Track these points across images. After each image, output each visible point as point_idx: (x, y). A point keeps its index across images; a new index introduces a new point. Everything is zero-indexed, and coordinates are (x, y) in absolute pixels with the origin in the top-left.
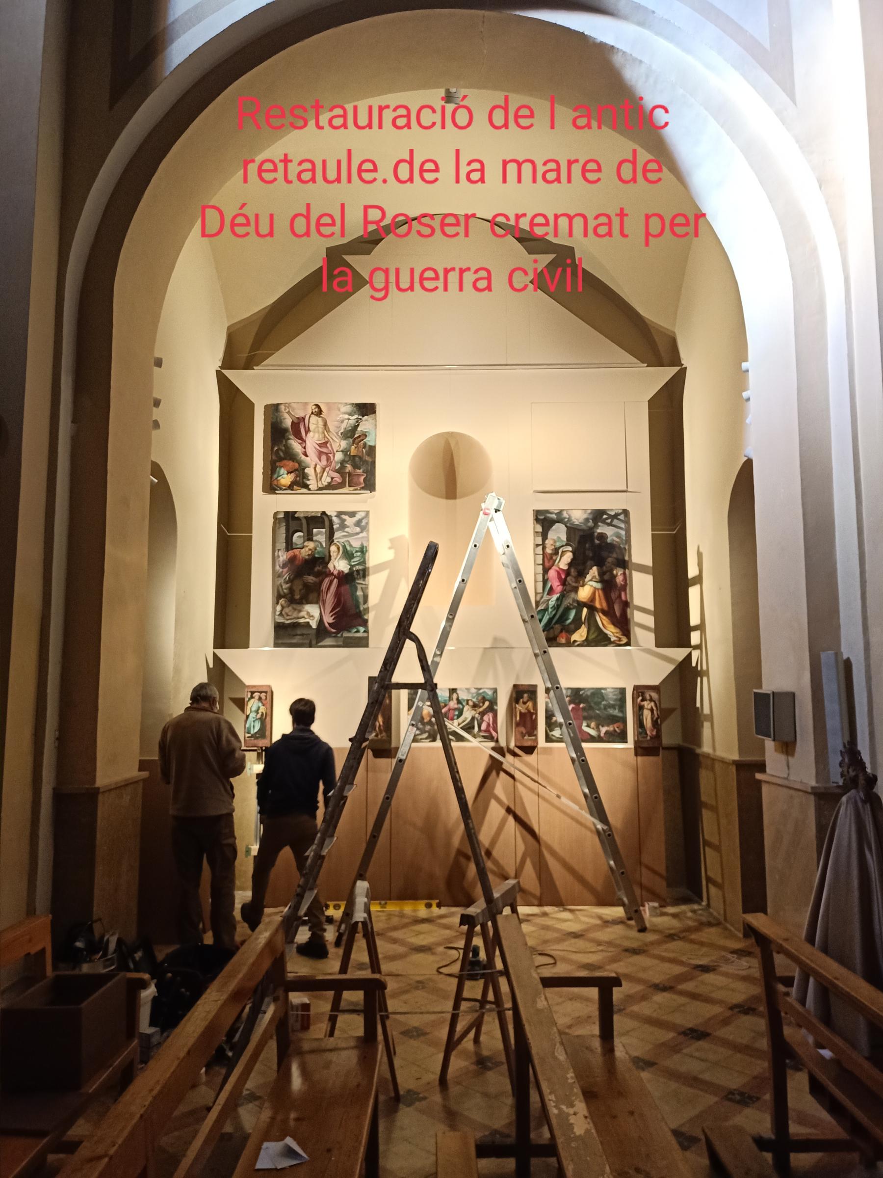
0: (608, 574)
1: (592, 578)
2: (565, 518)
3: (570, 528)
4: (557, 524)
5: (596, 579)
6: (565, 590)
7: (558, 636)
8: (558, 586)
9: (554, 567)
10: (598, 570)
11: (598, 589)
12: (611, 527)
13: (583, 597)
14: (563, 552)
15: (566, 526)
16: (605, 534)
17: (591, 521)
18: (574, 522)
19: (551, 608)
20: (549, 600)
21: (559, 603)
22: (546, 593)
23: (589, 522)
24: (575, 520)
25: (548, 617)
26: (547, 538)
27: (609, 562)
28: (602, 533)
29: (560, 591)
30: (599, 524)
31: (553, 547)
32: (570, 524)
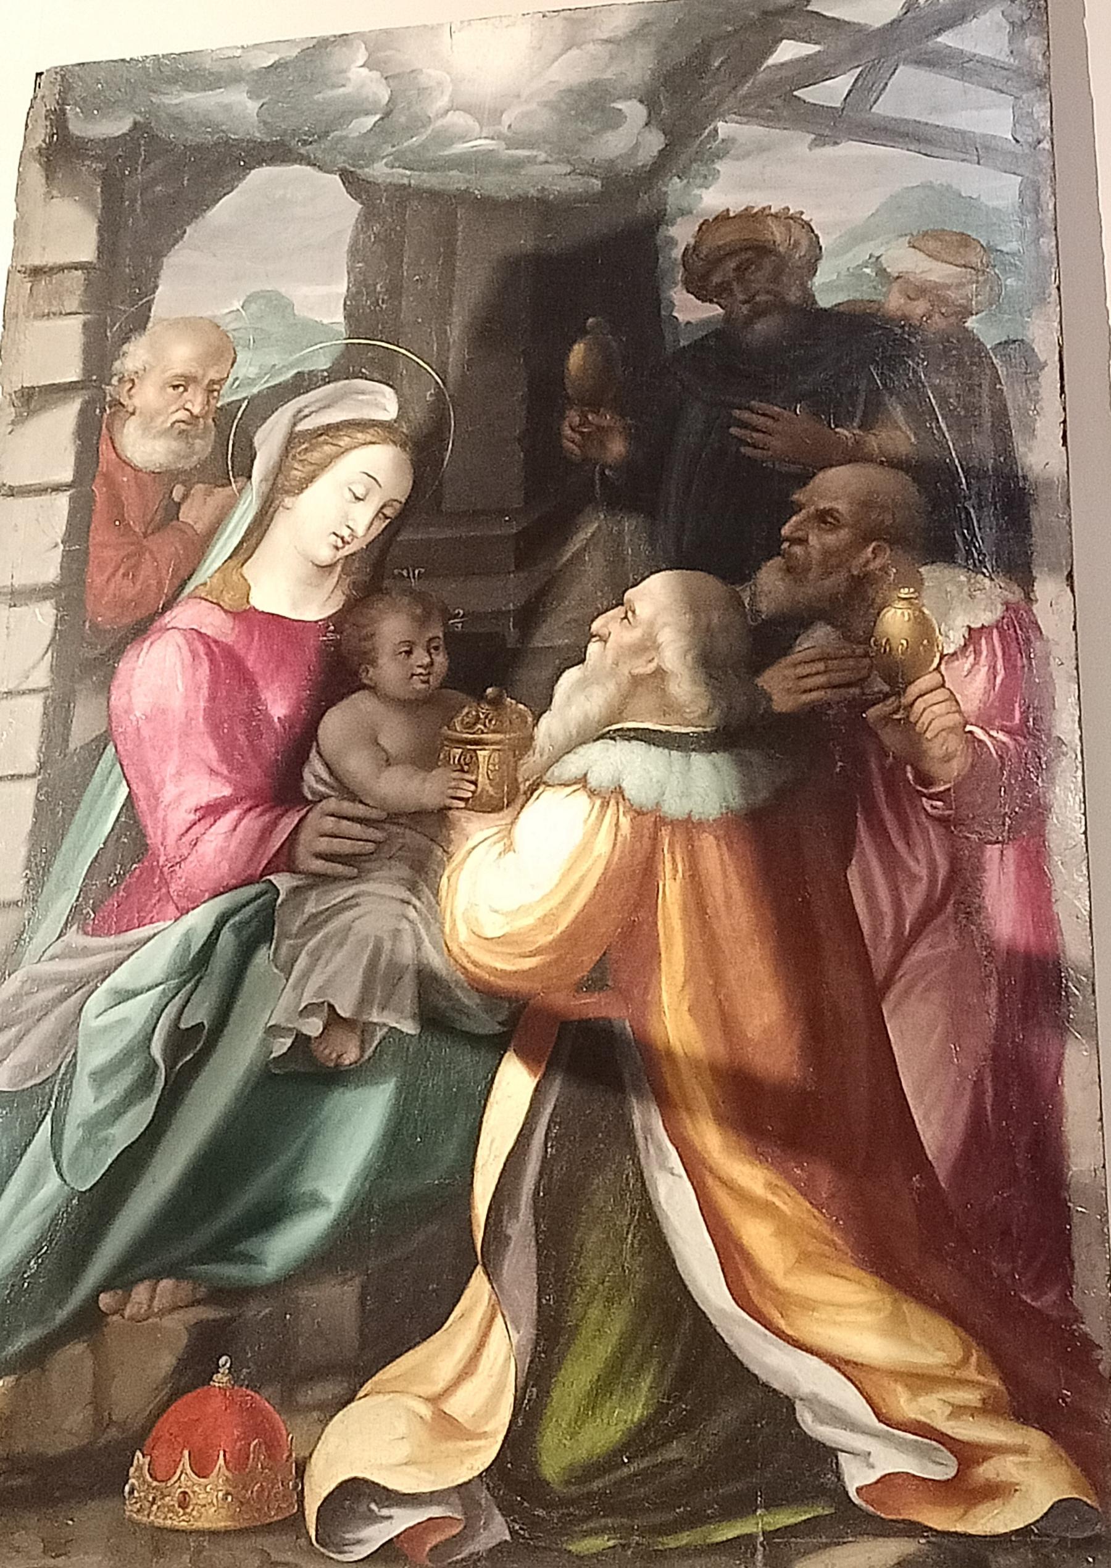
0: (820, 636)
1: (617, 713)
2: (356, 109)
3: (402, 194)
4: (260, 175)
5: (667, 708)
6: (284, 860)
7: (138, 1440)
8: (213, 811)
9: (184, 615)
10: (694, 605)
11: (688, 827)
12: (851, 149)
13: (494, 928)
14: (292, 439)
15: (353, 183)
16: (787, 218)
17: (634, 111)
18: (445, 138)
19: (100, 1078)
20: (87, 983)
21: (199, 1014)
22: (65, 902)
23: (615, 120)
24: (459, 120)
25: (52, 1185)
26: (140, 322)
27: (825, 518)
28: (749, 216)
29: (223, 870)
30: (724, 128)
31: (195, 402)
32: (400, 160)
